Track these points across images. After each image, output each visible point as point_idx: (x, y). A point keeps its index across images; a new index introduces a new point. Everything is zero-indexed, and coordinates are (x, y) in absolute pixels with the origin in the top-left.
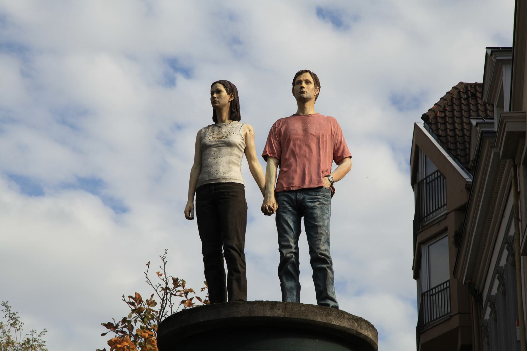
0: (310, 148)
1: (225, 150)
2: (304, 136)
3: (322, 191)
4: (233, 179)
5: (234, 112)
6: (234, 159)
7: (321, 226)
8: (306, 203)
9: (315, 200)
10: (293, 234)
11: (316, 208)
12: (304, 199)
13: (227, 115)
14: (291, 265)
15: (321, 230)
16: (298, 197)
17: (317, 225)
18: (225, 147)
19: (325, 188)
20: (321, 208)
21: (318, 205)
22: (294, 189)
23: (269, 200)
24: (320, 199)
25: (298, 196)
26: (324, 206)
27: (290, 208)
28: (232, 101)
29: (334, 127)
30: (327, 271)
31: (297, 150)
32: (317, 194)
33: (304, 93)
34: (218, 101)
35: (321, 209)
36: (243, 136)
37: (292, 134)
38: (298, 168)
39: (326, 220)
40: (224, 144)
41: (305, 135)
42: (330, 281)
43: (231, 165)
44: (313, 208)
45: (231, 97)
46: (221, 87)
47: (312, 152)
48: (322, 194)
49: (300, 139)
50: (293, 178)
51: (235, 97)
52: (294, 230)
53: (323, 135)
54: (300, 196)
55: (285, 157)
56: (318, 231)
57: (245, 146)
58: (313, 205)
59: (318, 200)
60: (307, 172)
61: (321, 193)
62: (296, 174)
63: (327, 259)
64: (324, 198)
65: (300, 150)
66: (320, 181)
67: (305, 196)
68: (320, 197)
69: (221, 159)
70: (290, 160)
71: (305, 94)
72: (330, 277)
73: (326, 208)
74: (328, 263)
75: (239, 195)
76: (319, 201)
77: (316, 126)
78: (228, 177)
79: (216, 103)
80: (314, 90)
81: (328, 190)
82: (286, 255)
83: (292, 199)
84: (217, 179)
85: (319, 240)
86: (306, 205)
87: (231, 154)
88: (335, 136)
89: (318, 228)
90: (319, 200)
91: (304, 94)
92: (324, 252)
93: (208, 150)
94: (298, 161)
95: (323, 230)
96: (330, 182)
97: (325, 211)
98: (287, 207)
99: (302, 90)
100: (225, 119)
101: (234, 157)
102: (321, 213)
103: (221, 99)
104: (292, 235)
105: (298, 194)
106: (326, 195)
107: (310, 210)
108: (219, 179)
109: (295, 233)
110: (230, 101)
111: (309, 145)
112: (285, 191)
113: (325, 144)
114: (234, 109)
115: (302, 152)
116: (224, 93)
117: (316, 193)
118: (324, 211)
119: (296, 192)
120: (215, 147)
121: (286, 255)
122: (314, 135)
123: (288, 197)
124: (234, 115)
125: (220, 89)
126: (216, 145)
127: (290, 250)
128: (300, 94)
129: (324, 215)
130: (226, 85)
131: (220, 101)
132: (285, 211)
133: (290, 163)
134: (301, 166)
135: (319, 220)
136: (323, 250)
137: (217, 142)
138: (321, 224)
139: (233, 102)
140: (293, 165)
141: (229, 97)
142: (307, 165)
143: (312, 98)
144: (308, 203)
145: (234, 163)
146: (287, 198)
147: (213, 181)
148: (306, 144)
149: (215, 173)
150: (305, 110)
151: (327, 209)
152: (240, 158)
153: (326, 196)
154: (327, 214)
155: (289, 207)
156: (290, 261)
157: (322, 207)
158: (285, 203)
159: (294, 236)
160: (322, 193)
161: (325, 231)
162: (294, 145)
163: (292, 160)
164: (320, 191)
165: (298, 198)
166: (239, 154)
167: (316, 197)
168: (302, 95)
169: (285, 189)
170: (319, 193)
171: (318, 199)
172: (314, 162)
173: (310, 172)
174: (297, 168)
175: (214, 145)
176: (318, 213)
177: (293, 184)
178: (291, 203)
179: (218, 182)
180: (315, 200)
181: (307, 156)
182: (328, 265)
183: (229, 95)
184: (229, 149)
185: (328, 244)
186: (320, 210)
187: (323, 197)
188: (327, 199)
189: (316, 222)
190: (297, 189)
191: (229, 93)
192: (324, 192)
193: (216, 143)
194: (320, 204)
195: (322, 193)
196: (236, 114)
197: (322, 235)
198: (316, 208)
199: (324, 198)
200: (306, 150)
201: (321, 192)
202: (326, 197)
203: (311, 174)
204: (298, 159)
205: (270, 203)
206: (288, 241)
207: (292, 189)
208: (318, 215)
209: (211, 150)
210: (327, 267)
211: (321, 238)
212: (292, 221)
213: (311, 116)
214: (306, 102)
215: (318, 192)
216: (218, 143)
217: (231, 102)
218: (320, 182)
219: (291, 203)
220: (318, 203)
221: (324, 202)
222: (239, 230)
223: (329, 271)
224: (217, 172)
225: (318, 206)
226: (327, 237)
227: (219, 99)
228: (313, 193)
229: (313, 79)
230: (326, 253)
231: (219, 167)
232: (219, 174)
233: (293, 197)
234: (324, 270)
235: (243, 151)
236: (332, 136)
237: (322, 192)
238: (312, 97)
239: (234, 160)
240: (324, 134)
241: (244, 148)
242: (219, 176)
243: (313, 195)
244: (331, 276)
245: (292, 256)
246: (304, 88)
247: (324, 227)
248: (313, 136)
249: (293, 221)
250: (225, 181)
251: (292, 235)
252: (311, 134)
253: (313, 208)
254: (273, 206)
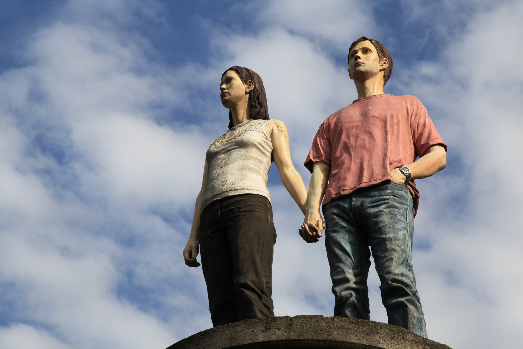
0: (371, 135)
1: (237, 153)
2: (362, 122)
3: (389, 188)
4: (247, 189)
5: (255, 107)
6: (250, 163)
7: (391, 238)
8: (367, 209)
9: (380, 203)
10: (351, 261)
11: (381, 214)
12: (362, 204)
13: (245, 113)
14: (350, 309)
15: (392, 244)
16: (353, 203)
17: (384, 238)
18: (236, 150)
19: (395, 183)
20: (390, 213)
21: (385, 208)
22: (346, 193)
23: (310, 217)
24: (388, 199)
25: (354, 202)
26: (395, 209)
27: (344, 224)
28: (250, 92)
29: (412, 105)
30: (407, 307)
31: (352, 141)
32: (381, 193)
33: (360, 65)
34: (228, 93)
35: (390, 214)
36: (266, 133)
37: (345, 123)
38: (352, 164)
39: (401, 230)
40: (236, 145)
41: (364, 119)
42: (415, 323)
43: (245, 172)
44: (377, 215)
45: (248, 87)
46: (232, 74)
47: (374, 140)
48: (390, 193)
49: (356, 127)
50: (345, 179)
51: (255, 87)
52: (353, 255)
53: (392, 116)
54: (356, 202)
55: (335, 156)
56: (388, 247)
57: (271, 148)
58: (376, 210)
59: (384, 202)
60: (365, 167)
61: (388, 191)
62: (350, 172)
63: (405, 288)
64: (393, 199)
65: (356, 141)
66: (385, 173)
67: (364, 200)
68: (388, 197)
69: (230, 165)
71: (362, 66)
72: (414, 317)
73: (399, 213)
74: (408, 295)
75: (256, 210)
76: (386, 203)
77: (381, 106)
78: (239, 187)
79: (226, 96)
81: (401, 187)
82: (340, 293)
83: (345, 207)
84: (223, 192)
85: (390, 259)
86: (367, 212)
87: (246, 158)
88: (413, 117)
89: (387, 242)
90: (387, 201)
91: (360, 67)
92: (400, 278)
93: (214, 160)
94: (353, 156)
95: (395, 244)
96: (403, 175)
97: (399, 217)
98: (338, 222)
99: (357, 62)
100: (243, 118)
101: (251, 161)
102: (390, 221)
103: (231, 90)
104: (348, 263)
105: (353, 199)
106: (397, 194)
107: (374, 219)
108: (226, 191)
109: (354, 259)
110: (248, 91)
111: (369, 131)
112: (333, 200)
113: (395, 127)
114: (255, 102)
115: (359, 142)
116: (237, 81)
117: (380, 192)
118: (396, 217)
119: (349, 197)
120: (223, 153)
121: (340, 293)
122: (377, 118)
123: (339, 207)
124: (255, 111)
125: (230, 77)
126: (224, 149)
127: (346, 285)
128: (355, 68)
129: (396, 223)
130: (240, 71)
131: (230, 93)
132: (337, 229)
133: (341, 161)
134: (358, 161)
135: (387, 230)
136: (398, 275)
137: (225, 145)
138: (391, 235)
139: (252, 94)
140: (345, 163)
141: (246, 86)
142: (366, 158)
143: (376, 74)
144: (369, 210)
145: (250, 169)
146: (338, 210)
147: (217, 198)
148: (365, 131)
149: (221, 185)
150: (366, 91)
151: (403, 215)
152: (261, 163)
153: (397, 196)
154: (403, 222)
155: (342, 222)
156: (348, 302)
157: (393, 212)
158: (335, 217)
159: (353, 264)
160: (390, 191)
161: (400, 246)
162: (348, 136)
163: (345, 156)
164: (387, 189)
165: (353, 204)
166: (259, 158)
167: (381, 197)
168: (357, 69)
169: (334, 196)
170: (385, 191)
171: (384, 199)
172: (378, 152)
173: (371, 167)
174: (351, 164)
175: (222, 150)
176: (385, 220)
177: (344, 186)
178: (345, 216)
179: (224, 196)
180: (380, 203)
181: (367, 145)
182: (408, 298)
183: (246, 83)
184: (242, 151)
185: (408, 268)
186: (389, 216)
187: (392, 197)
188: (400, 200)
189: (383, 235)
190: (351, 191)
191: (245, 81)
192: (394, 189)
193: (224, 147)
194: (388, 207)
195: (390, 191)
196: (258, 110)
197: (394, 252)
198: (381, 214)
199: (394, 197)
200: (365, 139)
201: (388, 189)
202: (398, 197)
203: (372, 168)
204: (352, 153)
205: (312, 221)
206: (343, 272)
207: (342, 193)
208: (386, 223)
209: (217, 159)
210: (407, 300)
211: (392, 257)
212: (348, 243)
213: (375, 97)
214: (367, 80)
215: (384, 189)
216: (227, 146)
217: (250, 93)
218: (385, 176)
219: (345, 216)
220: (384, 206)
221: (396, 204)
222: (258, 260)
223: (411, 307)
224: (223, 183)
225: (384, 210)
226: (404, 256)
227: (229, 90)
228: (376, 193)
229: (376, 47)
230: (405, 280)
231: (226, 177)
232: (225, 185)
233: (346, 206)
234: (403, 306)
236: (408, 118)
237: (390, 190)
238: (375, 70)
239: (251, 166)
240: (394, 114)
241: (271, 151)
242: (226, 188)
243: (375, 196)
244: (415, 315)
245: (351, 294)
246: (359, 58)
247: (398, 240)
248: (375, 119)
249: (350, 243)
250: (235, 193)
251: (348, 263)
252: (373, 116)
253: (377, 215)
254: (317, 226)
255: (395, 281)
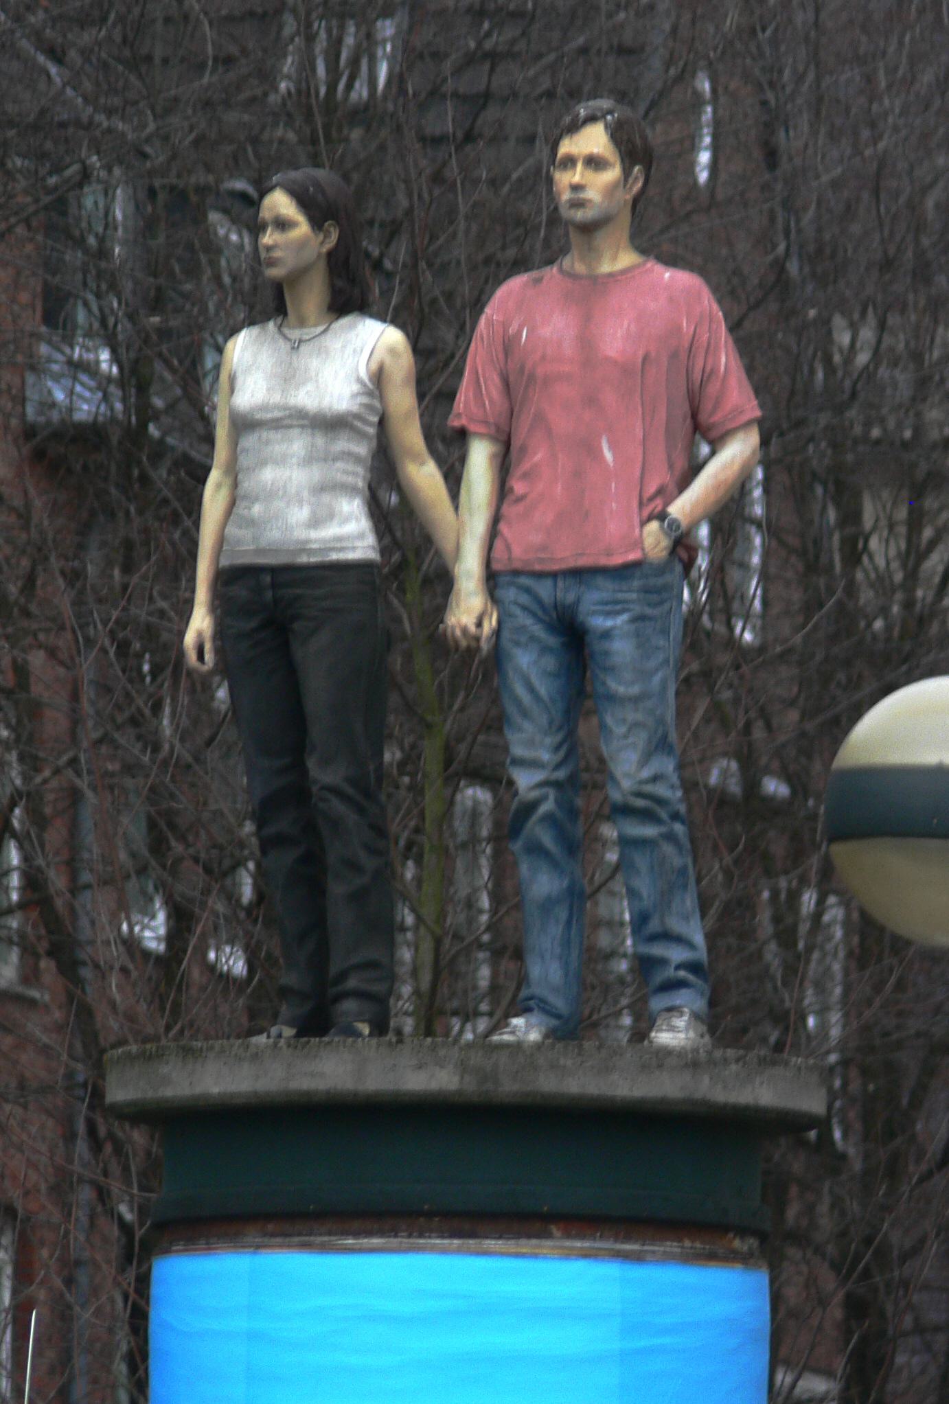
44: (607, 635)
54: (567, 594)
58: (609, 623)
59: (626, 606)
70: (535, 454)
78: (316, 541)
80: (622, 183)
92: (649, 788)
123: (528, 590)
180: (618, 607)
191: (317, 223)
235: (371, 431)
241: (375, 419)
255: (639, 794)
